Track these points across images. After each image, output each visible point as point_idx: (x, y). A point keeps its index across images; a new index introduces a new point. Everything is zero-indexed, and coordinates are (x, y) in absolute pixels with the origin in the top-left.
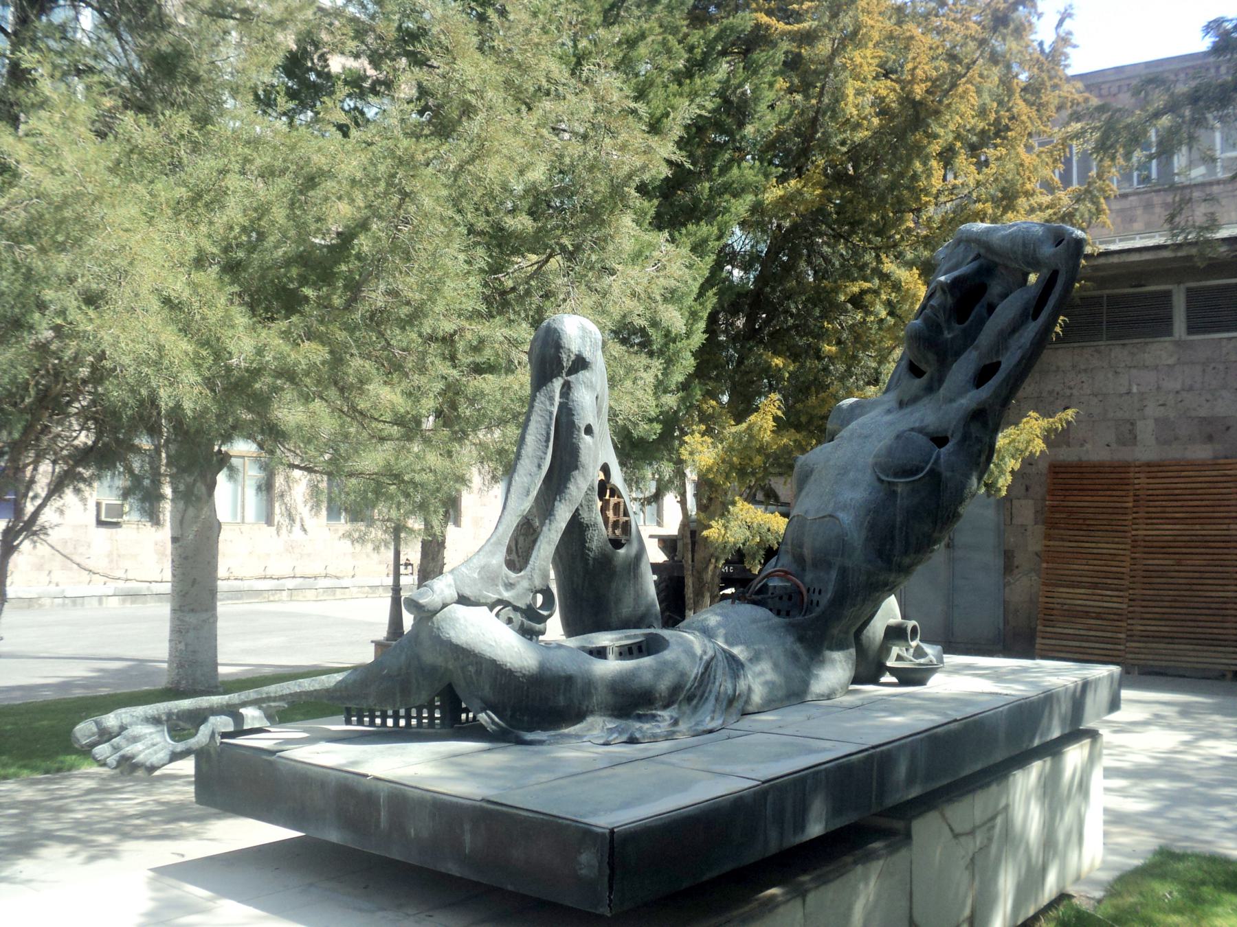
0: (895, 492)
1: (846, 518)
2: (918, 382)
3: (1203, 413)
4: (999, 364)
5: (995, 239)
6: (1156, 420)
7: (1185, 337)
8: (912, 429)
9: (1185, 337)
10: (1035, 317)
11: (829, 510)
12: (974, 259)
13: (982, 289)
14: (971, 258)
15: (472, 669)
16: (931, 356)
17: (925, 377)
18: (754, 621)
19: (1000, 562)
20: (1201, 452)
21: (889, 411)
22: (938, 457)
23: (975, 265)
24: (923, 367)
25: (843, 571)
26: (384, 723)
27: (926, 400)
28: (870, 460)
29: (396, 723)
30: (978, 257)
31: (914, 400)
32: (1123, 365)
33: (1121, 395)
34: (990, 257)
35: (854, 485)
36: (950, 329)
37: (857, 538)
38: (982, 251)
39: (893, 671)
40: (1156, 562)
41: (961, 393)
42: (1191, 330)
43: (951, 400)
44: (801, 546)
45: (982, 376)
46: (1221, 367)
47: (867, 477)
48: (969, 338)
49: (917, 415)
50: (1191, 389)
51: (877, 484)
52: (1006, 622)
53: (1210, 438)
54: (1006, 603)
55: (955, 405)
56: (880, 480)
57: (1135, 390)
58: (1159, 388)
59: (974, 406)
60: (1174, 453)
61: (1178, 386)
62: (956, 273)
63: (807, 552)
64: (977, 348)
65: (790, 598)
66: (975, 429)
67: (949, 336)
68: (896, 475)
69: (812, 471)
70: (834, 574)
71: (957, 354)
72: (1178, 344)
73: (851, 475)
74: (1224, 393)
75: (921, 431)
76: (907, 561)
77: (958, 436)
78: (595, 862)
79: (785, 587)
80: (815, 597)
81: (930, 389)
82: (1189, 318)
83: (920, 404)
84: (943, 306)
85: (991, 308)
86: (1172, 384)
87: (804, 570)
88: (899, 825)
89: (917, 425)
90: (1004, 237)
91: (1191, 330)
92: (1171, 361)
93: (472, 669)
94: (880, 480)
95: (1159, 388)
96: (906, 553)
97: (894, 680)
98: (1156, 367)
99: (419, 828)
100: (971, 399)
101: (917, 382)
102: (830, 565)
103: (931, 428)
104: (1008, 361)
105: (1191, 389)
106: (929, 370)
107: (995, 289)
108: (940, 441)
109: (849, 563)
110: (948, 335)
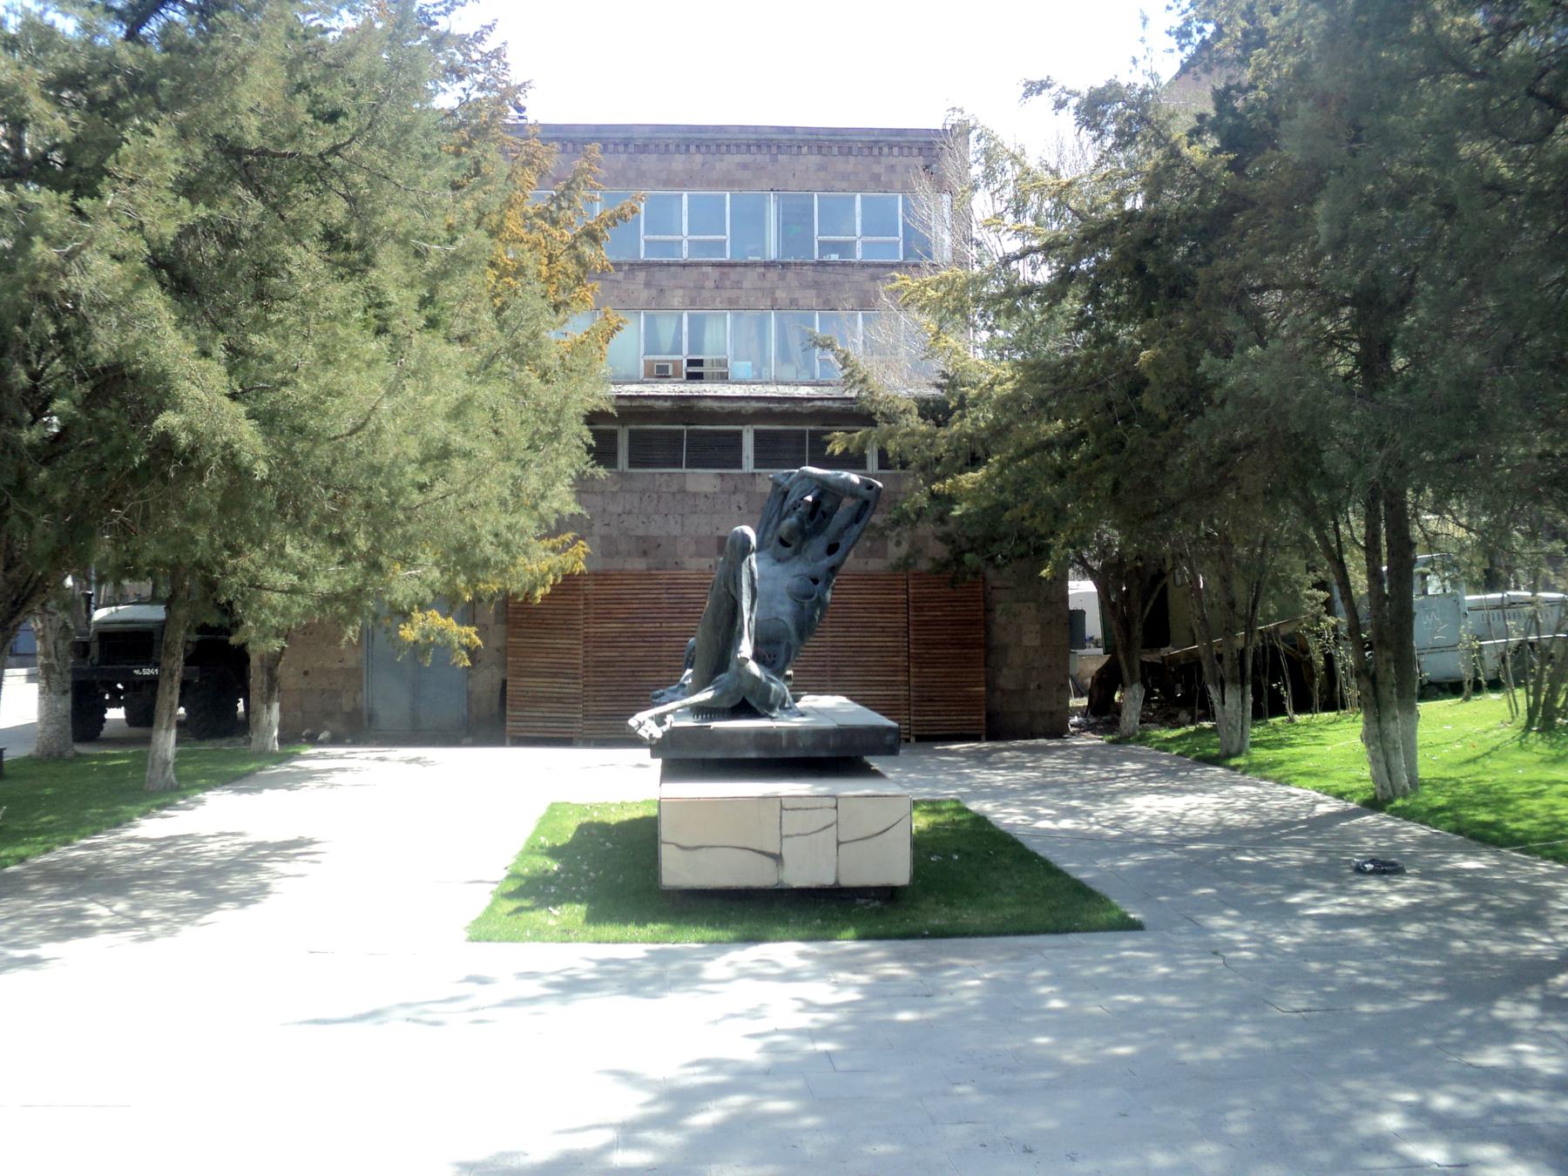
1: (786, 619)
2: (787, 551)
3: (640, 532)
5: (831, 480)
6: (602, 538)
7: (627, 470)
9: (627, 470)
20: (639, 564)
27: (796, 559)
35: (782, 602)
37: (792, 628)
40: (607, 654)
42: (632, 464)
45: (832, 549)
47: (788, 600)
50: (630, 513)
52: (469, 710)
53: (645, 553)
54: (469, 694)
60: (616, 564)
61: (620, 510)
72: (622, 475)
74: (656, 517)
82: (630, 455)
86: (615, 508)
91: (632, 464)
92: (616, 488)
98: (602, 493)
99: (809, 741)
100: (827, 562)
102: (779, 643)
105: (630, 513)
107: (826, 504)
108: (815, 581)
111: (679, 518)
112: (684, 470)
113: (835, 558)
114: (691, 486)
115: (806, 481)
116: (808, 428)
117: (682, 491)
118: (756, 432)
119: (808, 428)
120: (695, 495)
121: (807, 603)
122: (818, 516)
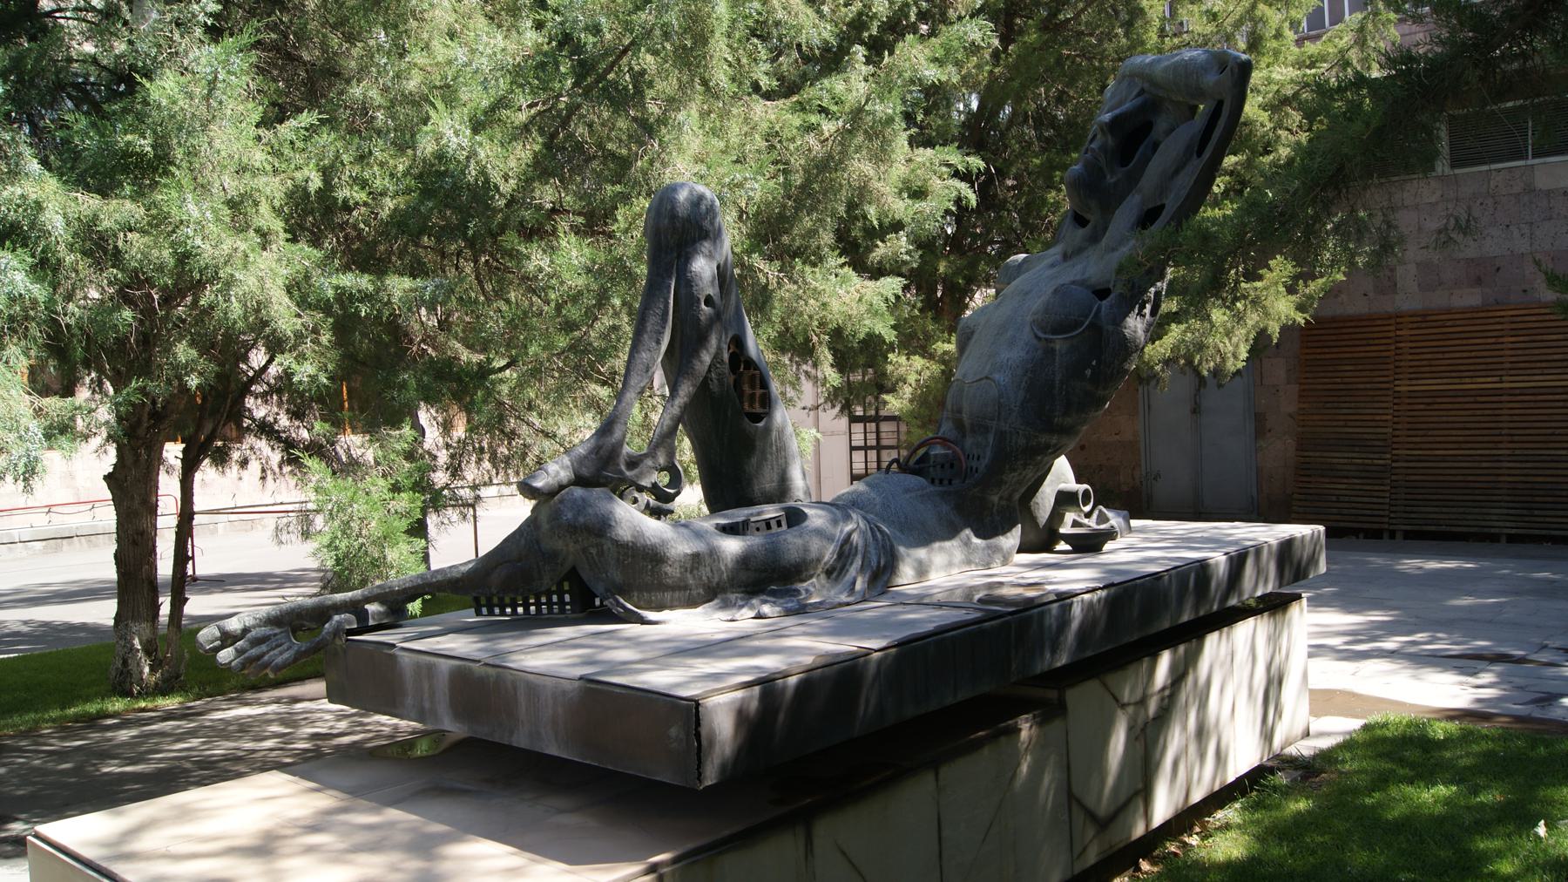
0: (1053, 350)
2: (1081, 232)
4: (1163, 206)
8: (1073, 282)
9: (1447, 171)
10: (1200, 153)
12: (1139, 95)
13: (1148, 127)
17: (1089, 226)
18: (907, 491)
20: (1470, 298)
22: (1099, 309)
23: (1139, 100)
24: (1088, 216)
25: (1001, 435)
26: (514, 611)
28: (1029, 318)
29: (527, 610)
30: (1142, 92)
31: (1078, 251)
38: (1146, 86)
39: (1068, 538)
42: (1456, 163)
43: (1113, 250)
44: (960, 411)
46: (1490, 201)
48: (1133, 180)
49: (1079, 267)
53: (1479, 281)
55: (1116, 254)
56: (1036, 337)
60: (1438, 300)
62: (1117, 112)
63: (965, 416)
65: (952, 466)
68: (1054, 332)
71: (1121, 199)
72: (1440, 178)
75: (1082, 283)
76: (1069, 421)
79: (946, 455)
80: (974, 464)
81: (1094, 239)
84: (1103, 148)
85: (1155, 146)
87: (964, 436)
88: (1052, 694)
89: (1078, 277)
90: (1167, 68)
91: (1456, 163)
92: (1433, 200)
93: (594, 551)
94: (1036, 337)
97: (1068, 547)
102: (987, 429)
104: (1171, 203)
106: (1093, 218)
107: (1161, 124)
110: (1110, 180)
111: (1526, 230)
112: (1530, 162)
114: (1542, 181)
117: (1530, 190)
120: (1549, 193)
121: (1060, 344)
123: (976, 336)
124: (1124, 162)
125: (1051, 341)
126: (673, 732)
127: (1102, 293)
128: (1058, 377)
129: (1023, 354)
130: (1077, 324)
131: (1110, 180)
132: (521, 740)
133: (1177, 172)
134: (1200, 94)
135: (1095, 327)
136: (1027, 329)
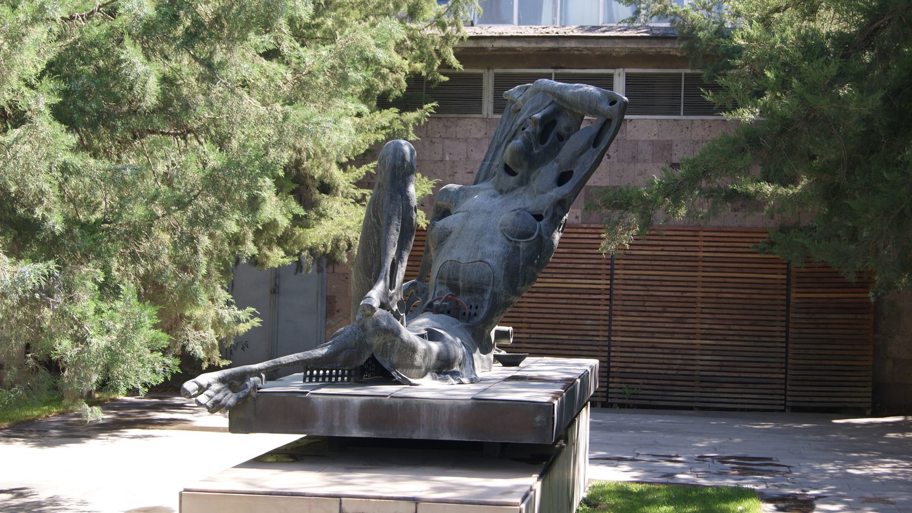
0: (518, 248)
7: (491, 115)
9: (491, 115)
11: (479, 256)
13: (554, 123)
14: (548, 103)
15: (389, 344)
16: (525, 164)
19: (322, 308)
21: (494, 196)
25: (494, 295)
27: (521, 190)
28: (498, 227)
30: (552, 102)
31: (511, 190)
32: (438, 136)
33: (435, 162)
34: (559, 102)
35: (492, 242)
36: (537, 147)
37: (500, 274)
38: (555, 99)
41: (550, 189)
43: (543, 193)
44: (457, 279)
45: (563, 179)
47: (499, 237)
48: (551, 153)
51: (507, 242)
56: (508, 239)
57: (447, 158)
58: (467, 158)
59: (559, 197)
63: (461, 284)
64: (557, 161)
66: (559, 210)
67: (537, 152)
68: (519, 237)
69: (450, 232)
70: (487, 296)
73: (488, 236)
75: (525, 209)
77: (550, 214)
78: (544, 419)
83: (516, 192)
84: (534, 132)
85: (561, 138)
90: (574, 94)
92: (479, 136)
93: (389, 344)
94: (511, 241)
95: (467, 158)
96: (523, 285)
98: (466, 140)
100: (557, 193)
101: (512, 178)
102: (483, 291)
103: (531, 209)
106: (520, 172)
107: (562, 124)
108: (539, 217)
109: (497, 290)
110: (536, 151)
113: (566, 189)
115: (540, 95)
116: (683, 71)
118: (629, 77)
119: (683, 71)
121: (522, 244)
122: (552, 136)
123: (452, 236)
124: (543, 142)
125: (519, 243)
126: (538, 418)
127: (539, 217)
128: (521, 264)
129: (501, 248)
130: (531, 234)
131: (536, 151)
132: (421, 434)
133: (581, 154)
134: (594, 112)
135: (540, 236)
136: (499, 235)
